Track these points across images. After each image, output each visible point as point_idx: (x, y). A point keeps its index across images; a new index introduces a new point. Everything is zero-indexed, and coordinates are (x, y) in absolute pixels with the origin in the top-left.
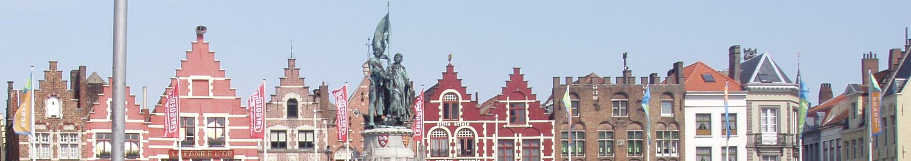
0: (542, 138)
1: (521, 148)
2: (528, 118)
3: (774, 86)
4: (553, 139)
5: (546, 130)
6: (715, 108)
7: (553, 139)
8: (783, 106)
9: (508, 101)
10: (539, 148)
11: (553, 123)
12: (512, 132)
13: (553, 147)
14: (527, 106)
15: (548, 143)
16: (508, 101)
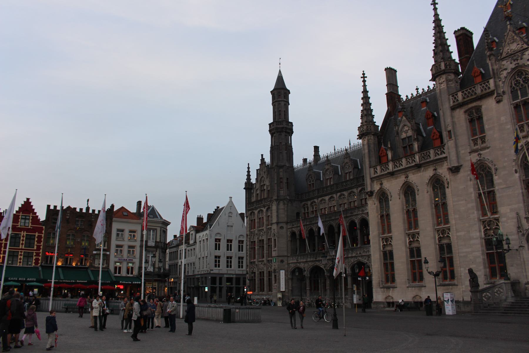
0: (37, 234)
1: (24, 239)
2: (30, 224)
3: (155, 219)
4: (43, 235)
5: (40, 230)
6: (127, 227)
7: (43, 235)
8: (159, 229)
9: (21, 214)
10: (34, 239)
11: (44, 227)
12: (21, 230)
13: (42, 239)
14: (31, 218)
15: (40, 237)
16: (21, 214)
